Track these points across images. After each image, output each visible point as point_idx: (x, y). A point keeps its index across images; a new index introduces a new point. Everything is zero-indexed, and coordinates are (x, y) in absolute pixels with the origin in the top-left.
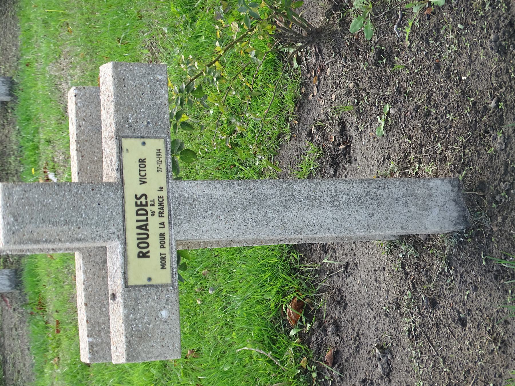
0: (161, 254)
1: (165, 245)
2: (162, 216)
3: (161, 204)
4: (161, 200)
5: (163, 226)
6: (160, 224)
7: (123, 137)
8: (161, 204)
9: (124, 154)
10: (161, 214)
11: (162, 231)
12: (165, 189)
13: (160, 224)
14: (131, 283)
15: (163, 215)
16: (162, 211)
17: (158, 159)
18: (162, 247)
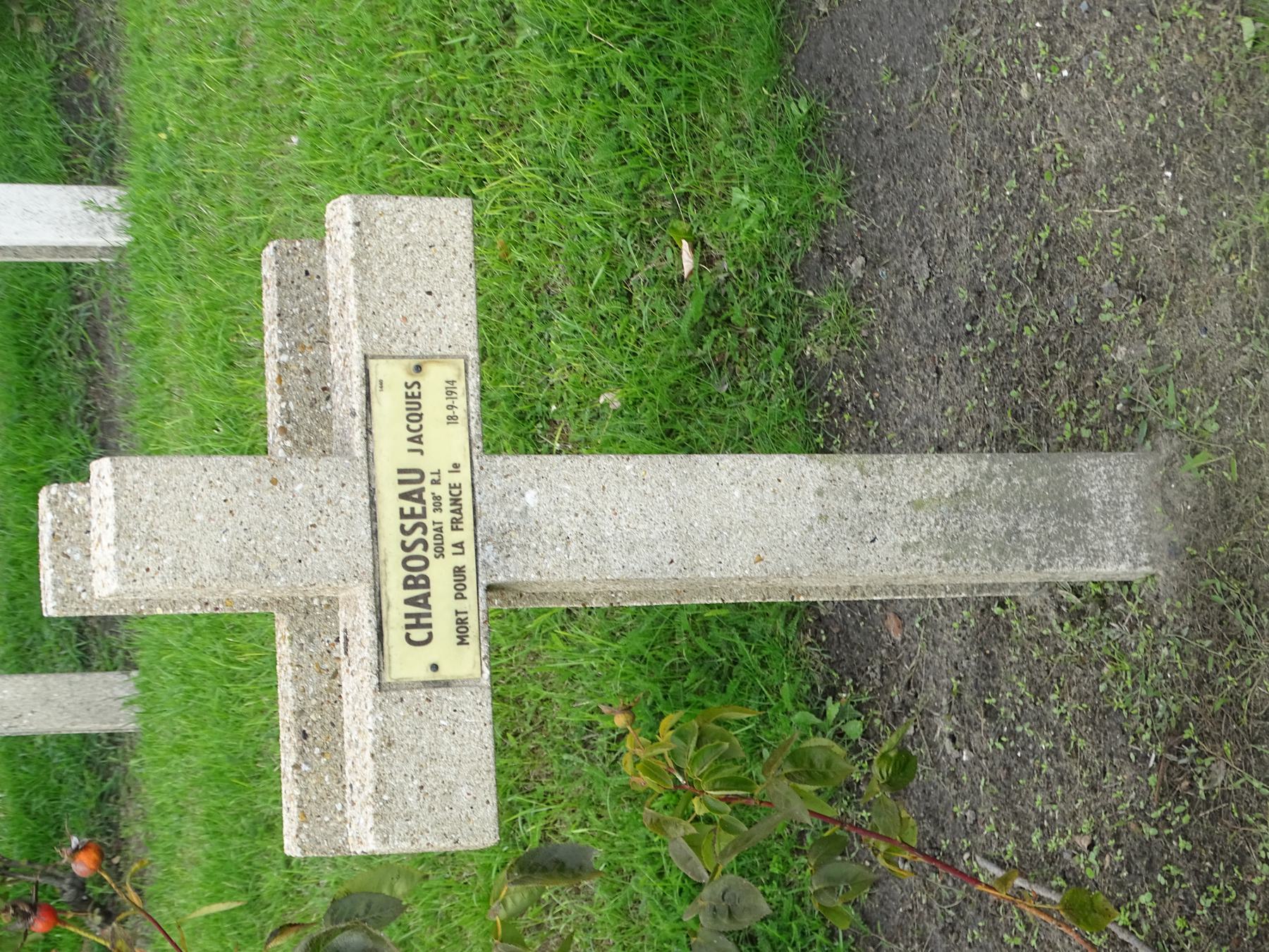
0: (457, 613)
2: (457, 529)
3: (456, 501)
4: (455, 491)
5: (460, 550)
6: (455, 545)
7: (373, 357)
8: (456, 501)
10: (456, 525)
11: (460, 560)
12: (465, 469)
13: (455, 545)
15: (460, 526)
16: (458, 516)
17: (450, 402)
18: (460, 596)
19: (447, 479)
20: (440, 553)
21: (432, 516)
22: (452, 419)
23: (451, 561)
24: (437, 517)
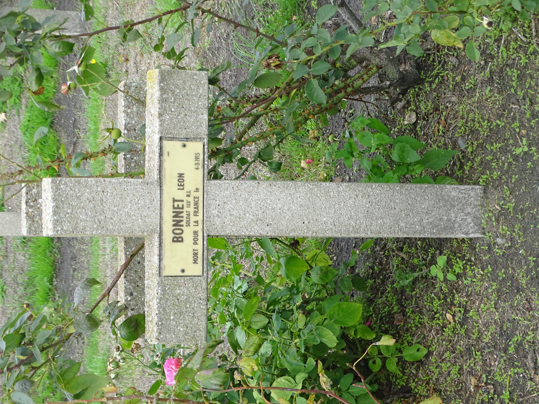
0: (194, 250)
1: (197, 242)
2: (196, 215)
3: (196, 204)
4: (196, 200)
5: (197, 224)
6: (195, 222)
8: (196, 204)
9: (165, 156)
10: (196, 213)
11: (196, 229)
13: (195, 222)
14: (165, 273)
16: (197, 210)
17: (196, 162)
18: (195, 243)
19: (193, 194)
20: (188, 225)
21: (185, 209)
22: (197, 169)
23: (192, 228)
24: (188, 209)
